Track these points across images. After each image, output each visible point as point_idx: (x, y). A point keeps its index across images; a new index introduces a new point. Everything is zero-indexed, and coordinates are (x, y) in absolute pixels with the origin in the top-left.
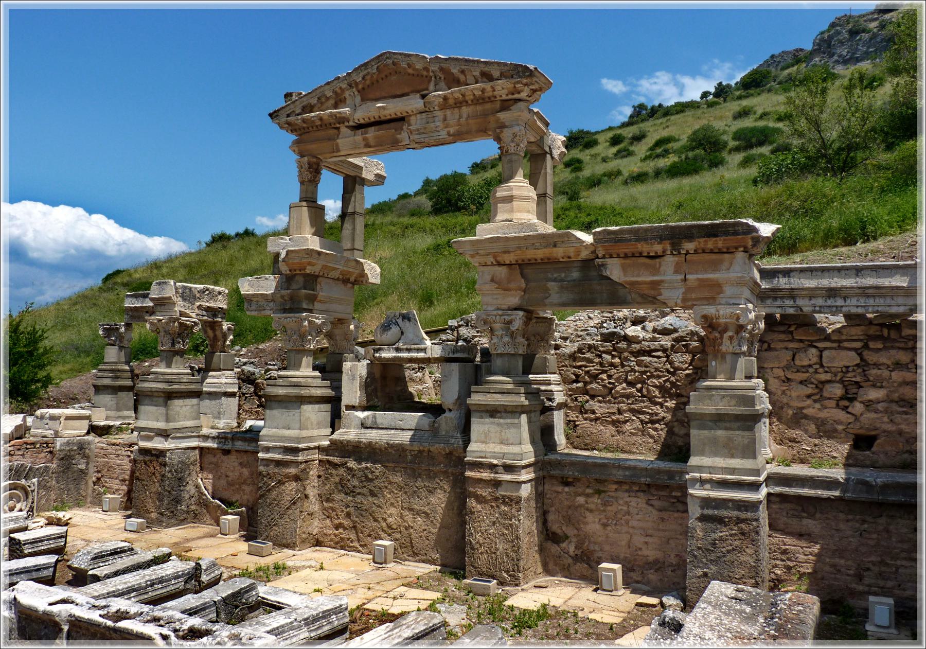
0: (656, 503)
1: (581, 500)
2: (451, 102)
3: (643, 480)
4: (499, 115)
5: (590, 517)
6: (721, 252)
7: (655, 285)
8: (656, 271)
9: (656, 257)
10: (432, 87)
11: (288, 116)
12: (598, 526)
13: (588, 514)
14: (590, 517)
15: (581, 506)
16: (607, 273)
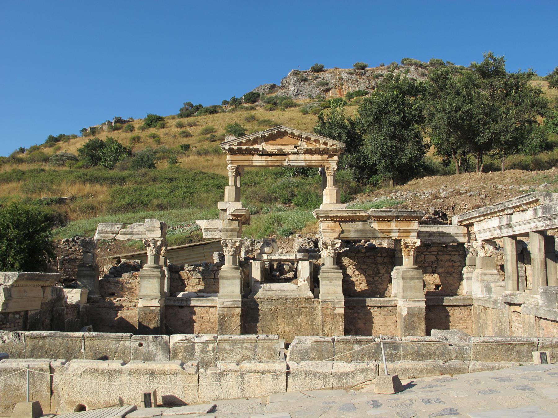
0: (383, 313)
1: (356, 315)
2: (309, 151)
3: (379, 305)
4: (329, 159)
5: (359, 321)
6: (411, 221)
7: (390, 231)
8: (390, 226)
9: (390, 221)
10: (299, 144)
11: (230, 146)
12: (362, 325)
13: (358, 320)
14: (359, 321)
15: (356, 317)
16: (372, 226)
